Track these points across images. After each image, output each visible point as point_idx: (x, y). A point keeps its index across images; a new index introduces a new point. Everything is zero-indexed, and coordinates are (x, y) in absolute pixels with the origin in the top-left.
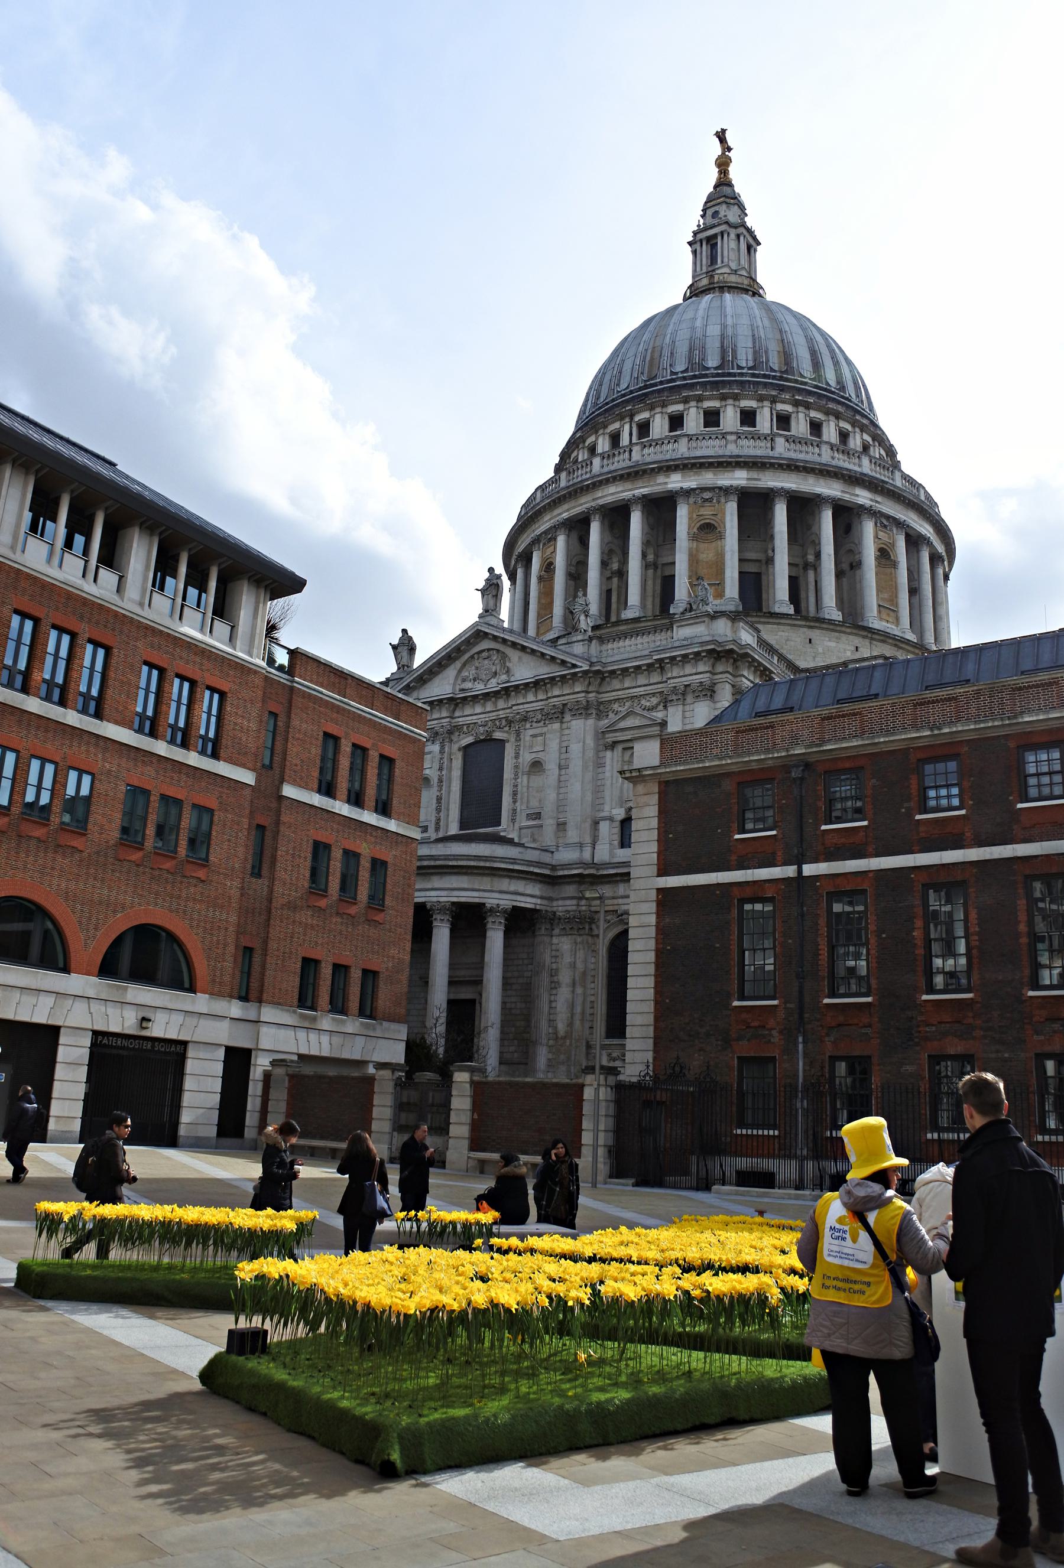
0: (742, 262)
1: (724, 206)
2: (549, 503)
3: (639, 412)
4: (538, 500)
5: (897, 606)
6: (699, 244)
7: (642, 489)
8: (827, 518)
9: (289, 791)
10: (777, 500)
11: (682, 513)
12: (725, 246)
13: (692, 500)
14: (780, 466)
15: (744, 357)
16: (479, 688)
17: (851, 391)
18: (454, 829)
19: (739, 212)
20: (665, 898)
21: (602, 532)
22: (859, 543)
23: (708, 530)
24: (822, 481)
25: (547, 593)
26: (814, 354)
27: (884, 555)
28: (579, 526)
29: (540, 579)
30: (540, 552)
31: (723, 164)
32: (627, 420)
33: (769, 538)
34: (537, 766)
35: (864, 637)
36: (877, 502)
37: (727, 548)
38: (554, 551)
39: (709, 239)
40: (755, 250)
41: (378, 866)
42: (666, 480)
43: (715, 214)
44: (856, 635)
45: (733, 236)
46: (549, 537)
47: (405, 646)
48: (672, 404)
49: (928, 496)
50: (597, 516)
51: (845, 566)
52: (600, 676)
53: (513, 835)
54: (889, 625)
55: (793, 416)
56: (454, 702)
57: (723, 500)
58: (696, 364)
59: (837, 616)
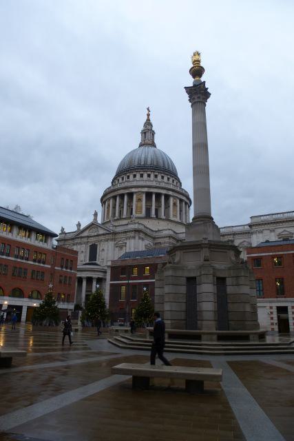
7: (127, 191)
8: (163, 197)
9: (56, 268)
11: (135, 196)
15: (149, 162)
16: (93, 234)
17: (171, 168)
18: (88, 262)
20: (111, 285)
23: (139, 200)
25: (108, 211)
26: (164, 164)
27: (175, 204)
28: (115, 198)
31: (148, 115)
33: (151, 201)
34: (103, 250)
41: (70, 278)
46: (109, 199)
47: (79, 225)
49: (185, 191)
52: (115, 233)
53: (98, 263)
56: (88, 237)
58: (139, 164)
59: (164, 217)
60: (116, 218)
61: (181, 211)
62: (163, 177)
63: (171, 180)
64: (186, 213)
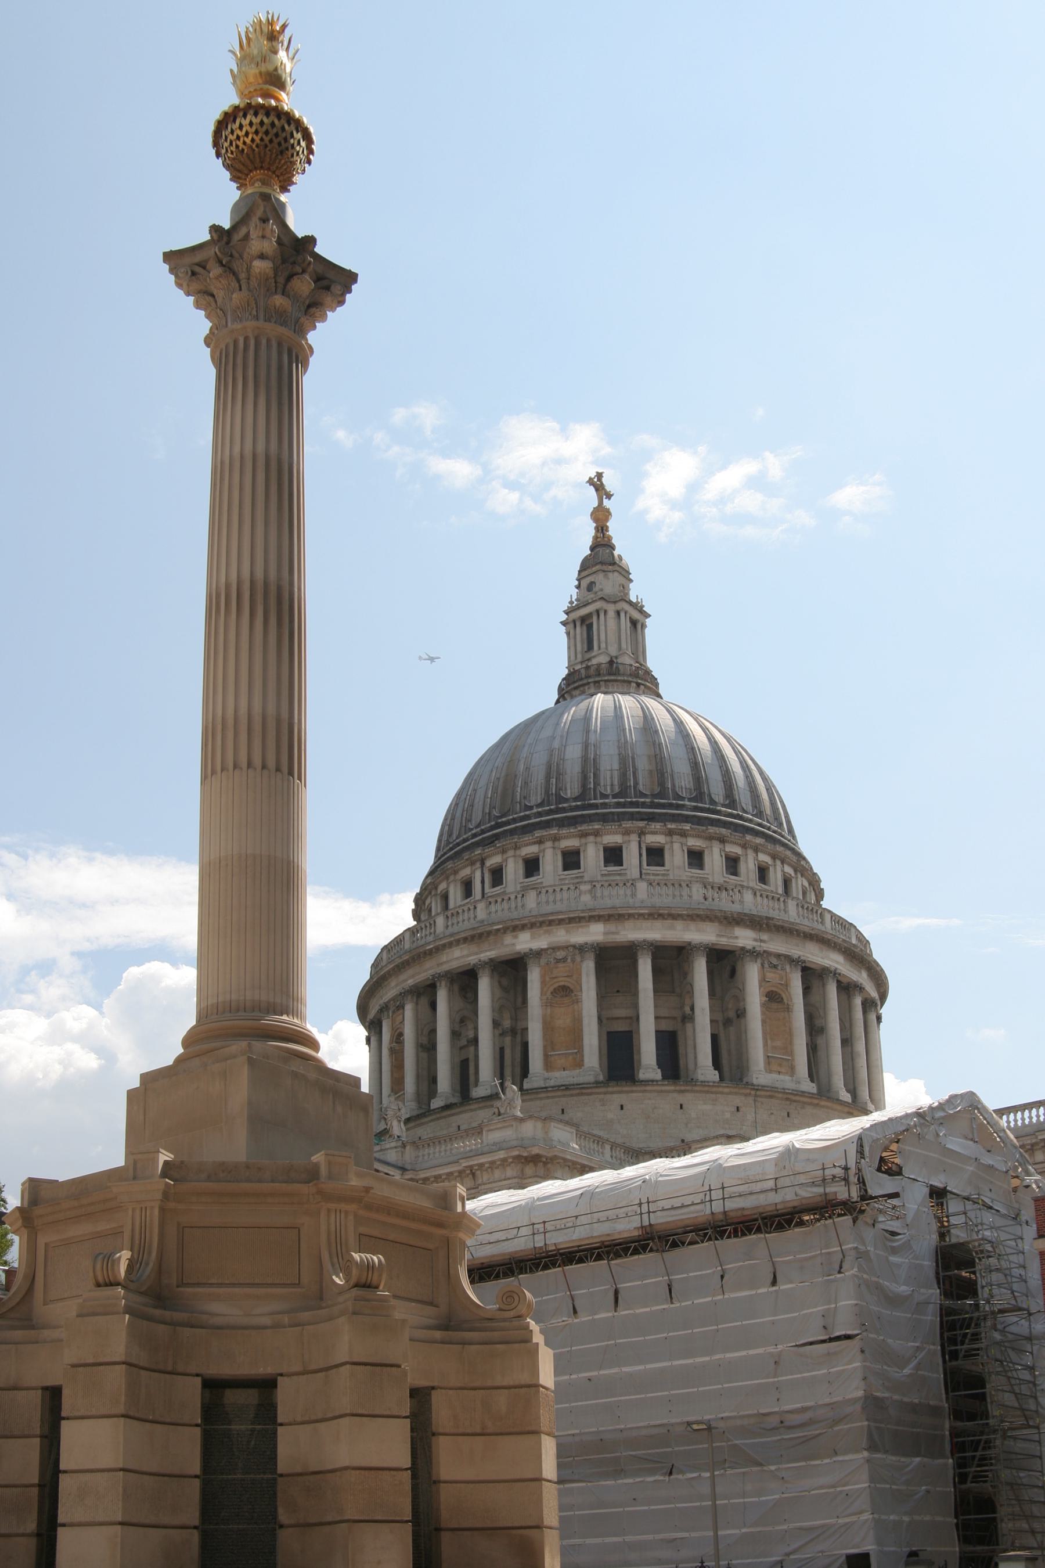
0: (624, 646)
1: (601, 575)
2: (393, 969)
3: (489, 856)
4: (384, 963)
5: (791, 1053)
6: (572, 625)
7: (489, 953)
8: (700, 971)
10: (639, 953)
11: (534, 977)
12: (602, 628)
13: (543, 961)
14: (641, 916)
19: (621, 580)
21: (450, 1001)
22: (742, 990)
24: (692, 925)
27: (774, 999)
28: (427, 991)
29: (392, 1051)
30: (390, 1020)
32: (478, 865)
35: (746, 1095)
36: (761, 941)
37: (585, 1013)
38: (402, 1022)
39: (583, 619)
40: (643, 626)
42: (514, 941)
43: (590, 587)
44: (736, 1094)
45: (611, 614)
46: (397, 1006)
48: (527, 845)
50: (443, 983)
51: (731, 1014)
54: (782, 1077)
55: (667, 847)
57: (578, 958)
60: (436, 1103)
61: (815, 1029)
62: (696, 858)
63: (748, 866)
64: (847, 1042)
